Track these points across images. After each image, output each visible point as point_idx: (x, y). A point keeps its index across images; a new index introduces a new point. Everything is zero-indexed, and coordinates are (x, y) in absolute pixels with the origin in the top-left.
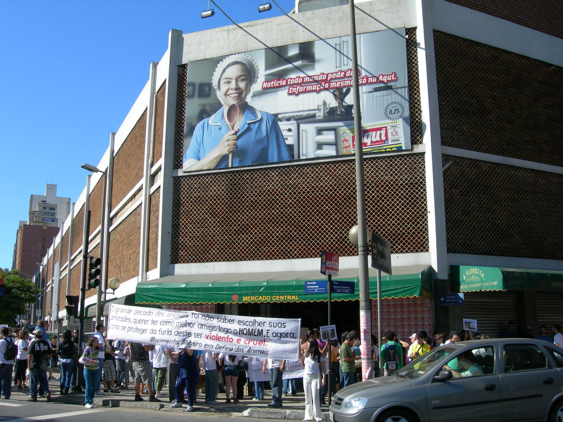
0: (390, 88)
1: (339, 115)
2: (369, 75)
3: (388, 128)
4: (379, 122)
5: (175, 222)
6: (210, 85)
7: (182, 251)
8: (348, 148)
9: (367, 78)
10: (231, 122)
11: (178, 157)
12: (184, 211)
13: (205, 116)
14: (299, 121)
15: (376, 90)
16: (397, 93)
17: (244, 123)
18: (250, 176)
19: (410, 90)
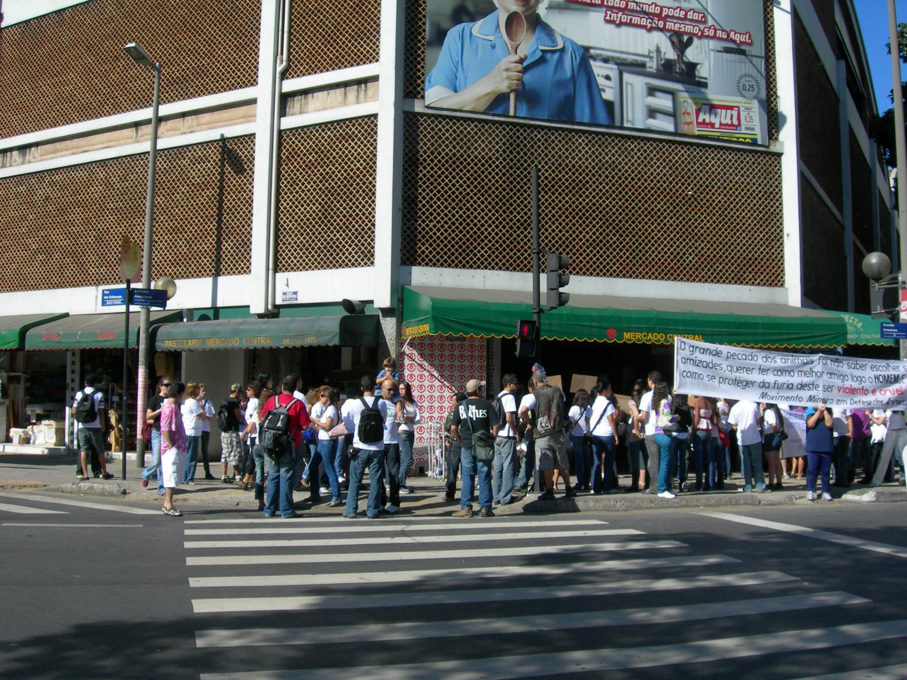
0: (742, 53)
1: (677, 73)
2: (718, 27)
3: (742, 109)
5: (409, 193)
7: (423, 244)
8: (691, 126)
9: (715, 30)
10: (511, 40)
11: (411, 77)
12: (425, 175)
13: (465, 18)
14: (622, 67)
15: (727, 50)
17: (534, 48)
18: (542, 136)
19: (766, 63)
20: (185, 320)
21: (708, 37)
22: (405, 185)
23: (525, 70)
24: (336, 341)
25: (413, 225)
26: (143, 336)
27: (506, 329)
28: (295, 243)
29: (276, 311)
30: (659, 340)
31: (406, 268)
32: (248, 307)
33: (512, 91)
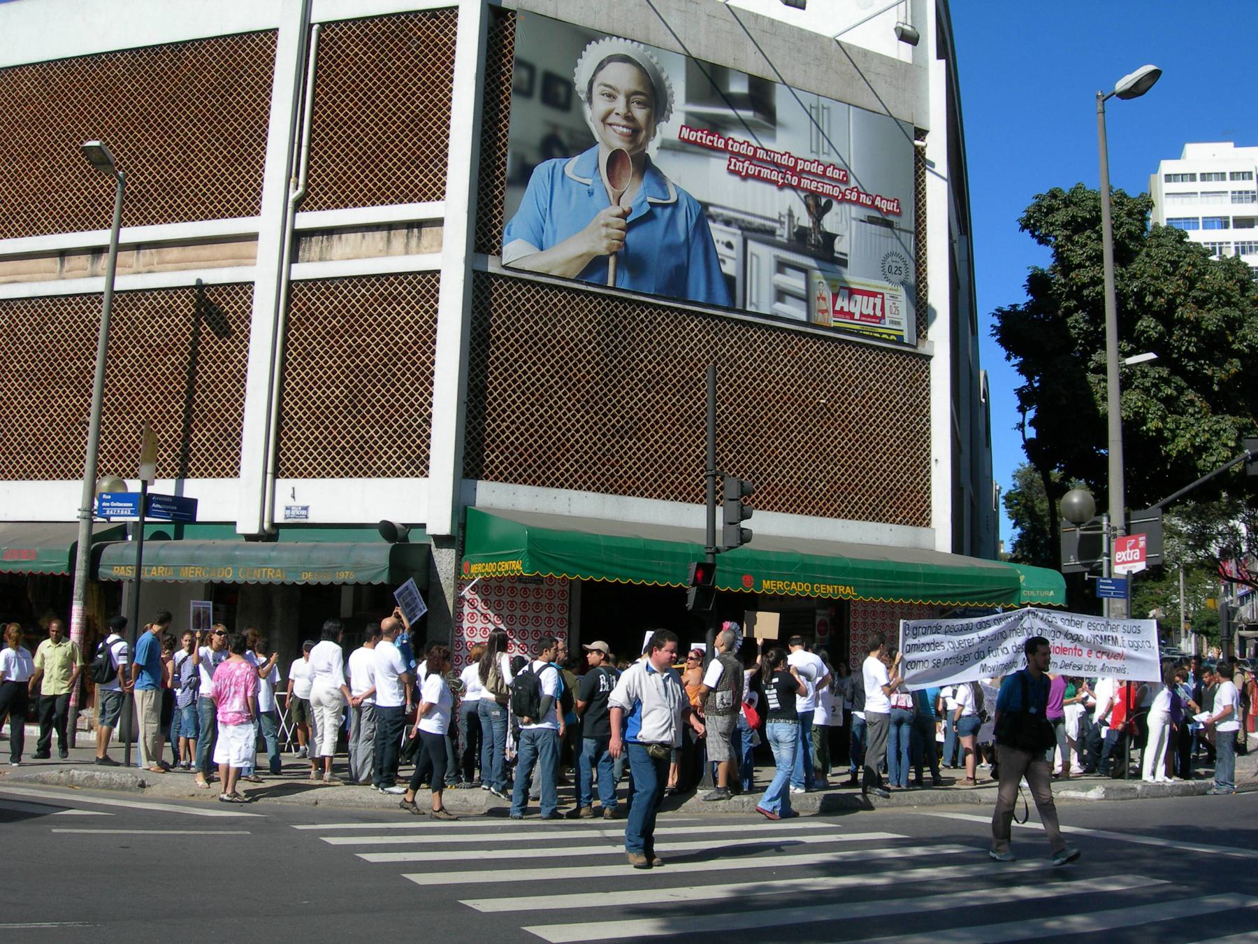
0: (889, 224)
3: (886, 297)
4: (873, 282)
6: (569, 85)
9: (859, 193)
13: (556, 151)
14: (746, 233)
15: (871, 220)
16: (899, 239)
20: (130, 538)
21: (850, 201)
22: (472, 370)
23: (629, 227)
24: (384, 578)
25: (480, 424)
26: (81, 557)
27: (619, 570)
28: (307, 438)
29: (274, 532)
30: (804, 592)
31: (470, 481)
32: (234, 523)
33: (611, 254)
